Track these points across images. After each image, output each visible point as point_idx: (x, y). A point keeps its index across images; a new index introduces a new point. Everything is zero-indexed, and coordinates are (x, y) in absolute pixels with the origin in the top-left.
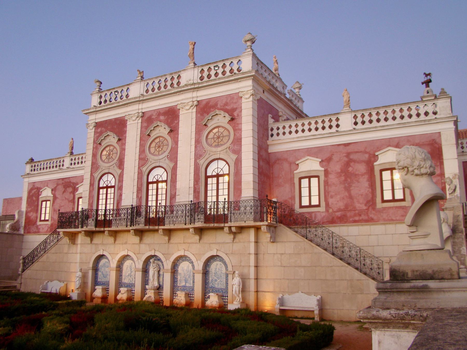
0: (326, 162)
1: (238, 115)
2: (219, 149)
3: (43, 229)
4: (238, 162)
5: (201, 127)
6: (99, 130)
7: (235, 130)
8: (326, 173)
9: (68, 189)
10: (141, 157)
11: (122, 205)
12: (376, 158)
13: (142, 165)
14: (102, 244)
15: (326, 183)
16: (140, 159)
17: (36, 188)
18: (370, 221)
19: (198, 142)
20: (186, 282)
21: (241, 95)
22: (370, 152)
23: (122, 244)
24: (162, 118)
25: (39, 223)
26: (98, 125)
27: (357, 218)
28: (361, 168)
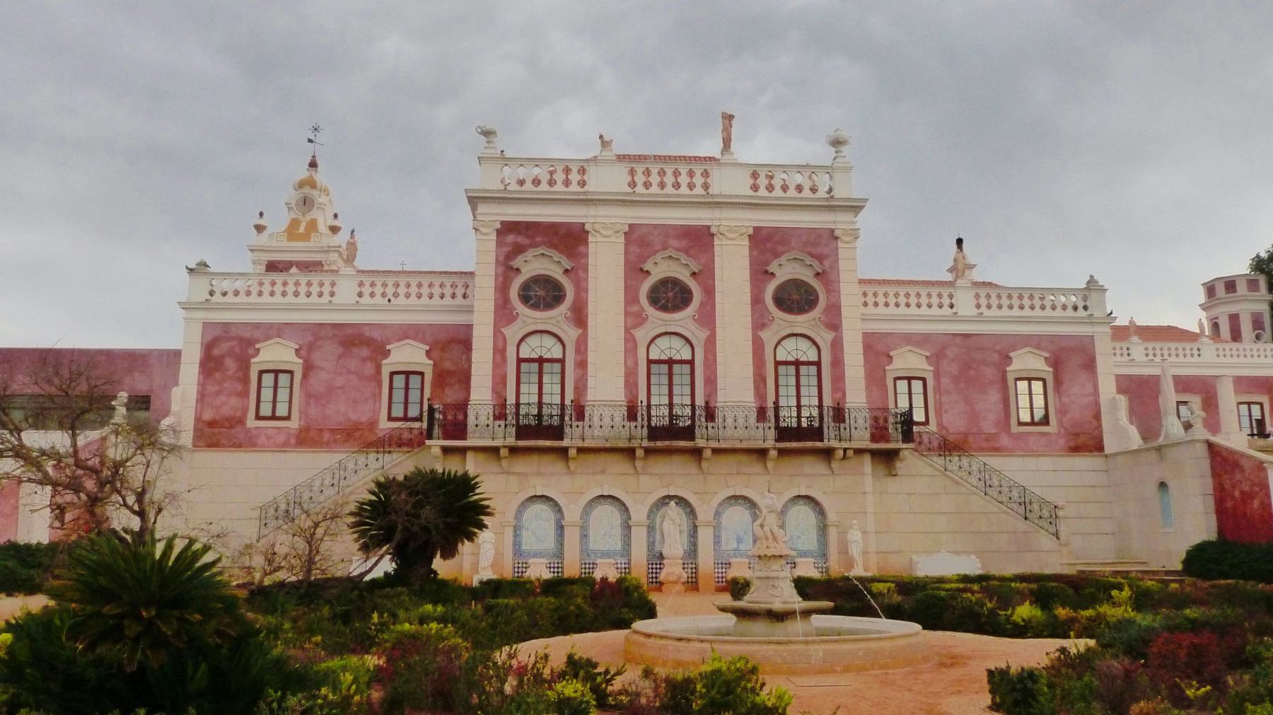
0: (936, 359)
1: (832, 267)
2: (800, 318)
3: (269, 438)
4: (837, 346)
5: (760, 274)
6: (510, 238)
7: (828, 291)
8: (937, 376)
9: (355, 350)
10: (629, 309)
11: (589, 398)
12: (1007, 360)
13: (635, 327)
14: (538, 474)
15: (938, 389)
16: (626, 314)
17: (234, 339)
18: (997, 450)
19: (757, 300)
20: (739, 541)
21: (837, 233)
22: (1002, 350)
23: (594, 474)
24: (674, 243)
25: (251, 422)
26: (508, 228)
27: (985, 445)
28: (989, 372)
